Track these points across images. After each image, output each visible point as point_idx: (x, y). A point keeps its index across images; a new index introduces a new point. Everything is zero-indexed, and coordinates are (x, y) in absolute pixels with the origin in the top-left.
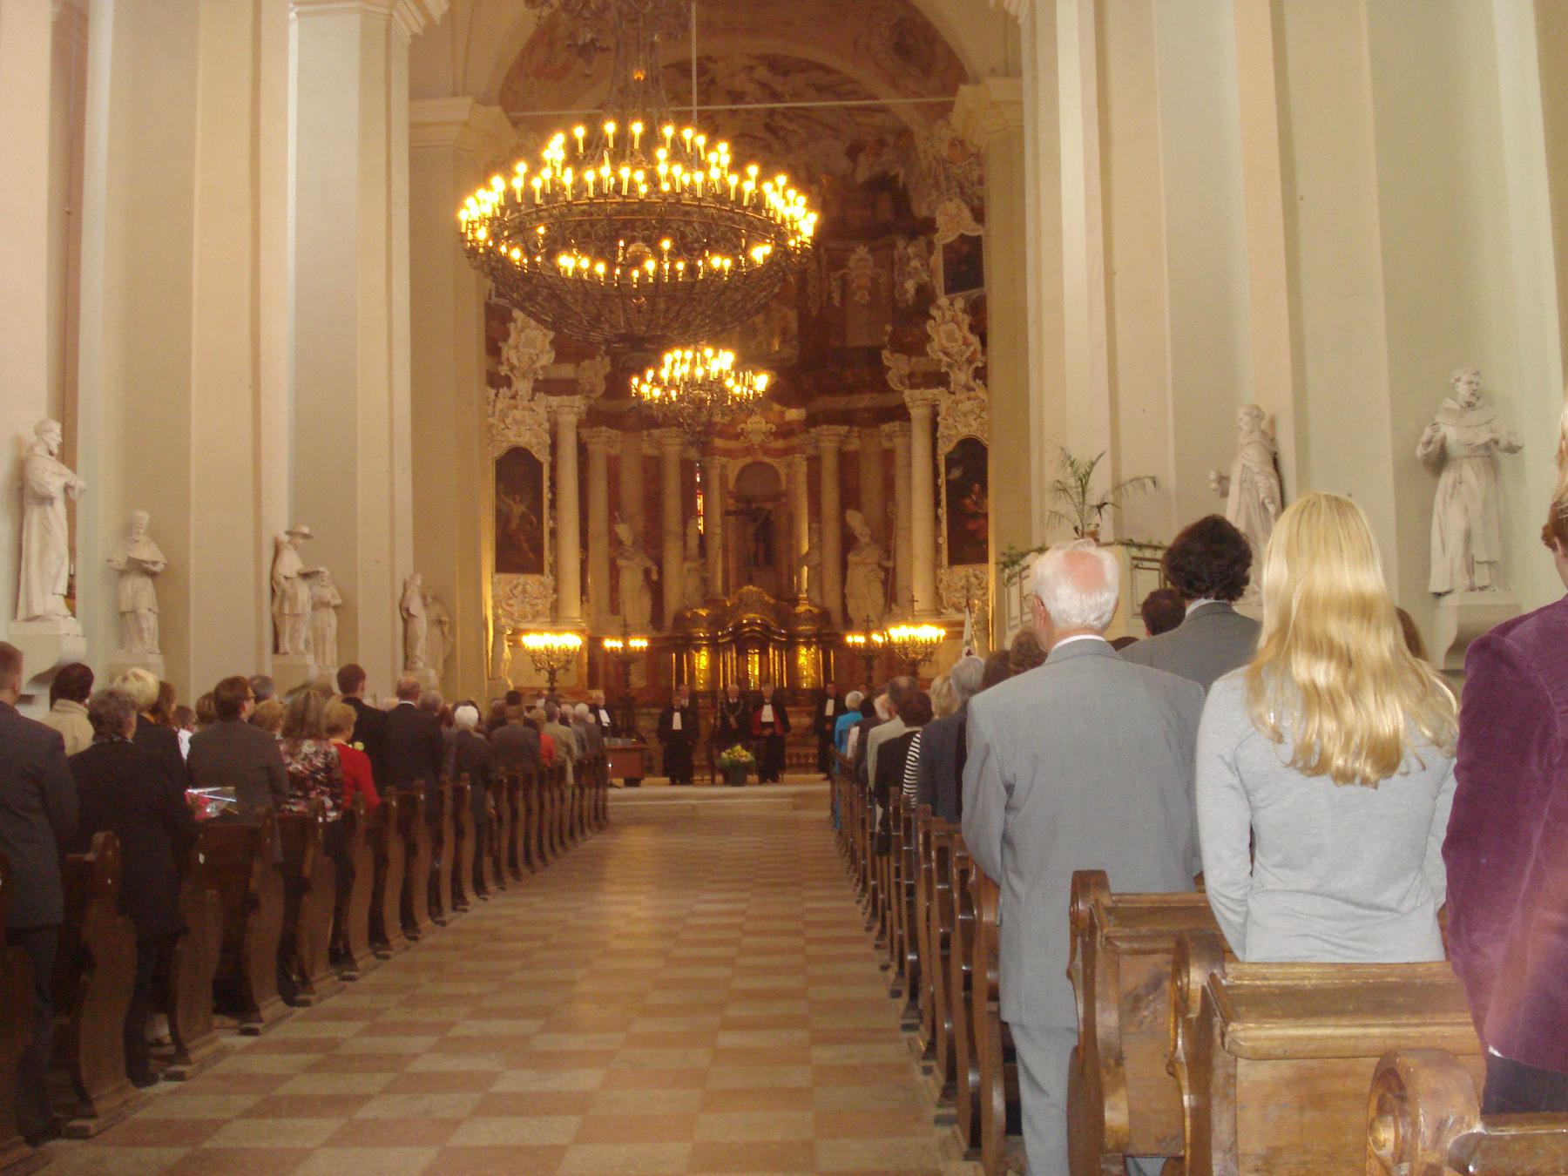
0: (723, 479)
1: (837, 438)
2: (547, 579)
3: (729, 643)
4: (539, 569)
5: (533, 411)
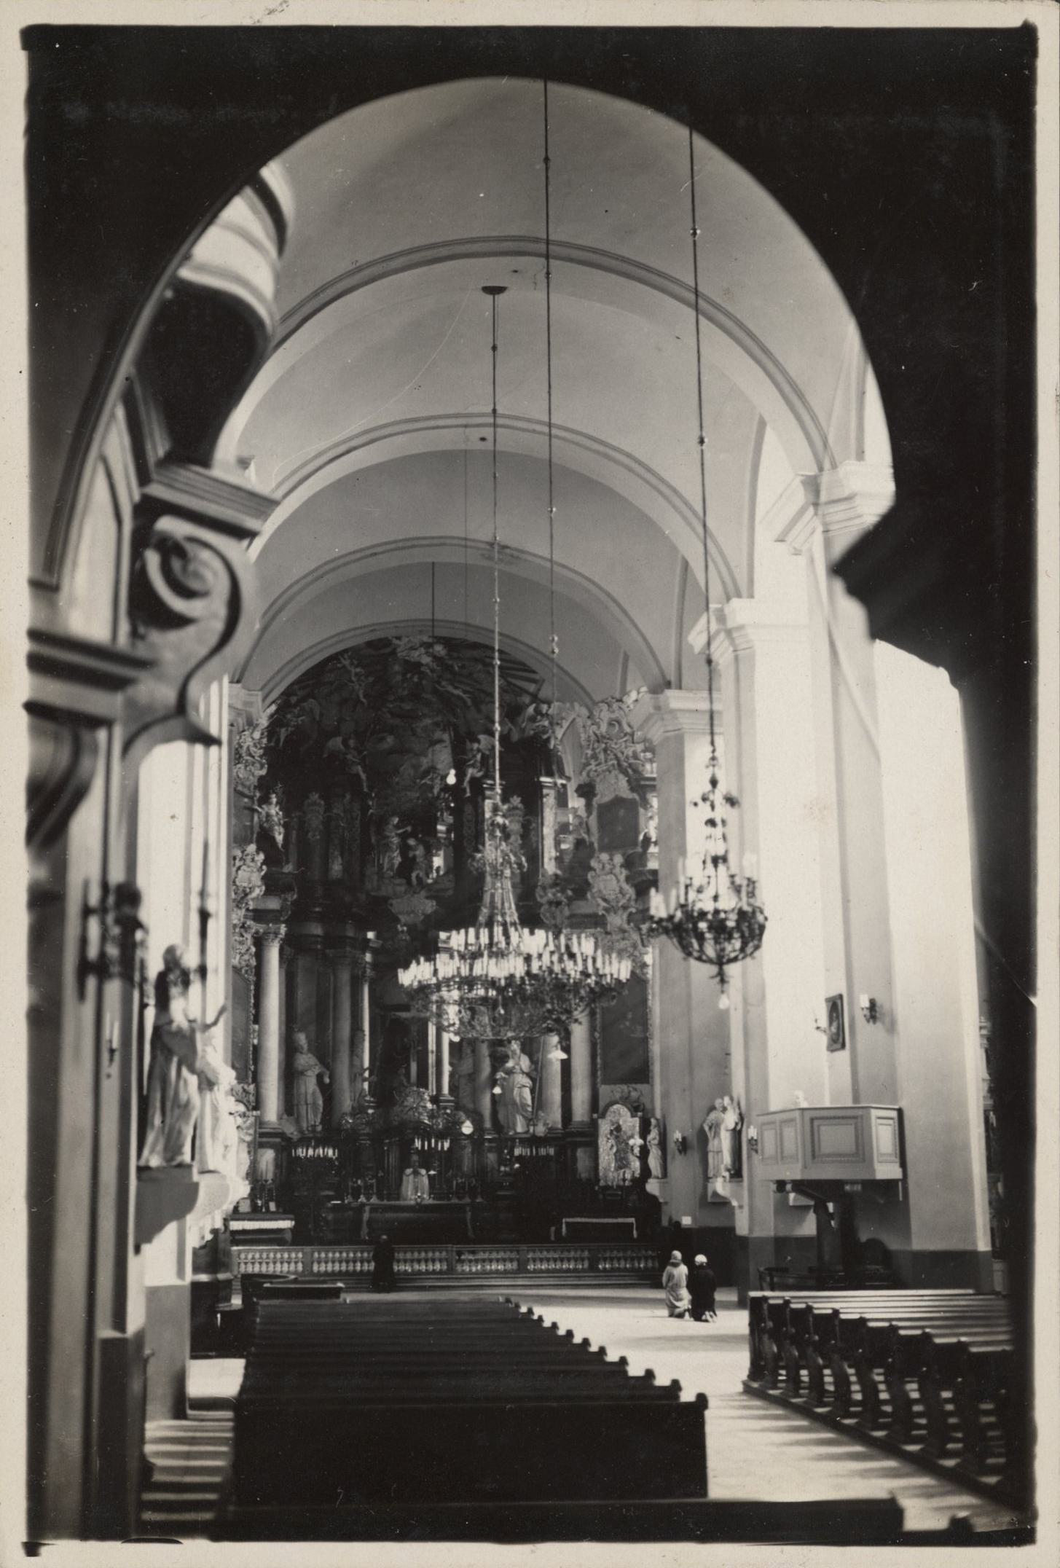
5: (243, 936)
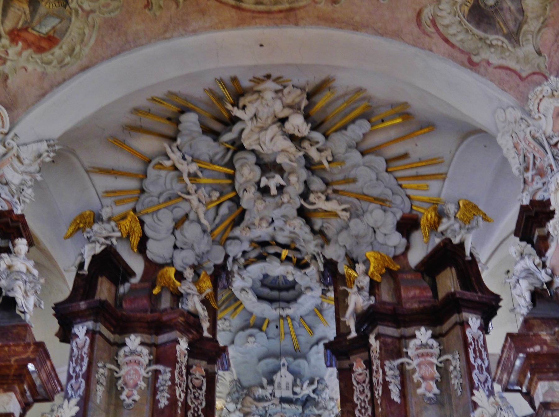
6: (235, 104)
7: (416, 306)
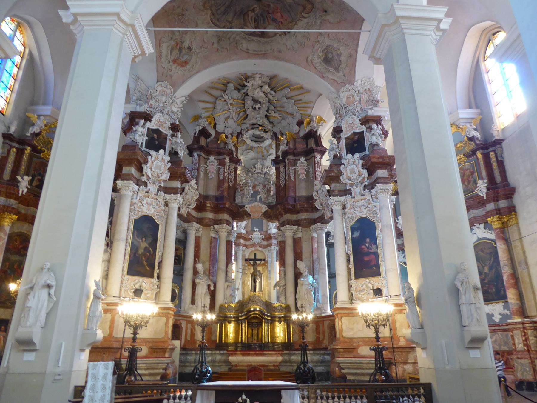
0: (243, 256)
1: (292, 231)
2: (155, 281)
3: (245, 319)
4: (152, 276)
5: (157, 200)
6: (246, 81)
7: (301, 150)
